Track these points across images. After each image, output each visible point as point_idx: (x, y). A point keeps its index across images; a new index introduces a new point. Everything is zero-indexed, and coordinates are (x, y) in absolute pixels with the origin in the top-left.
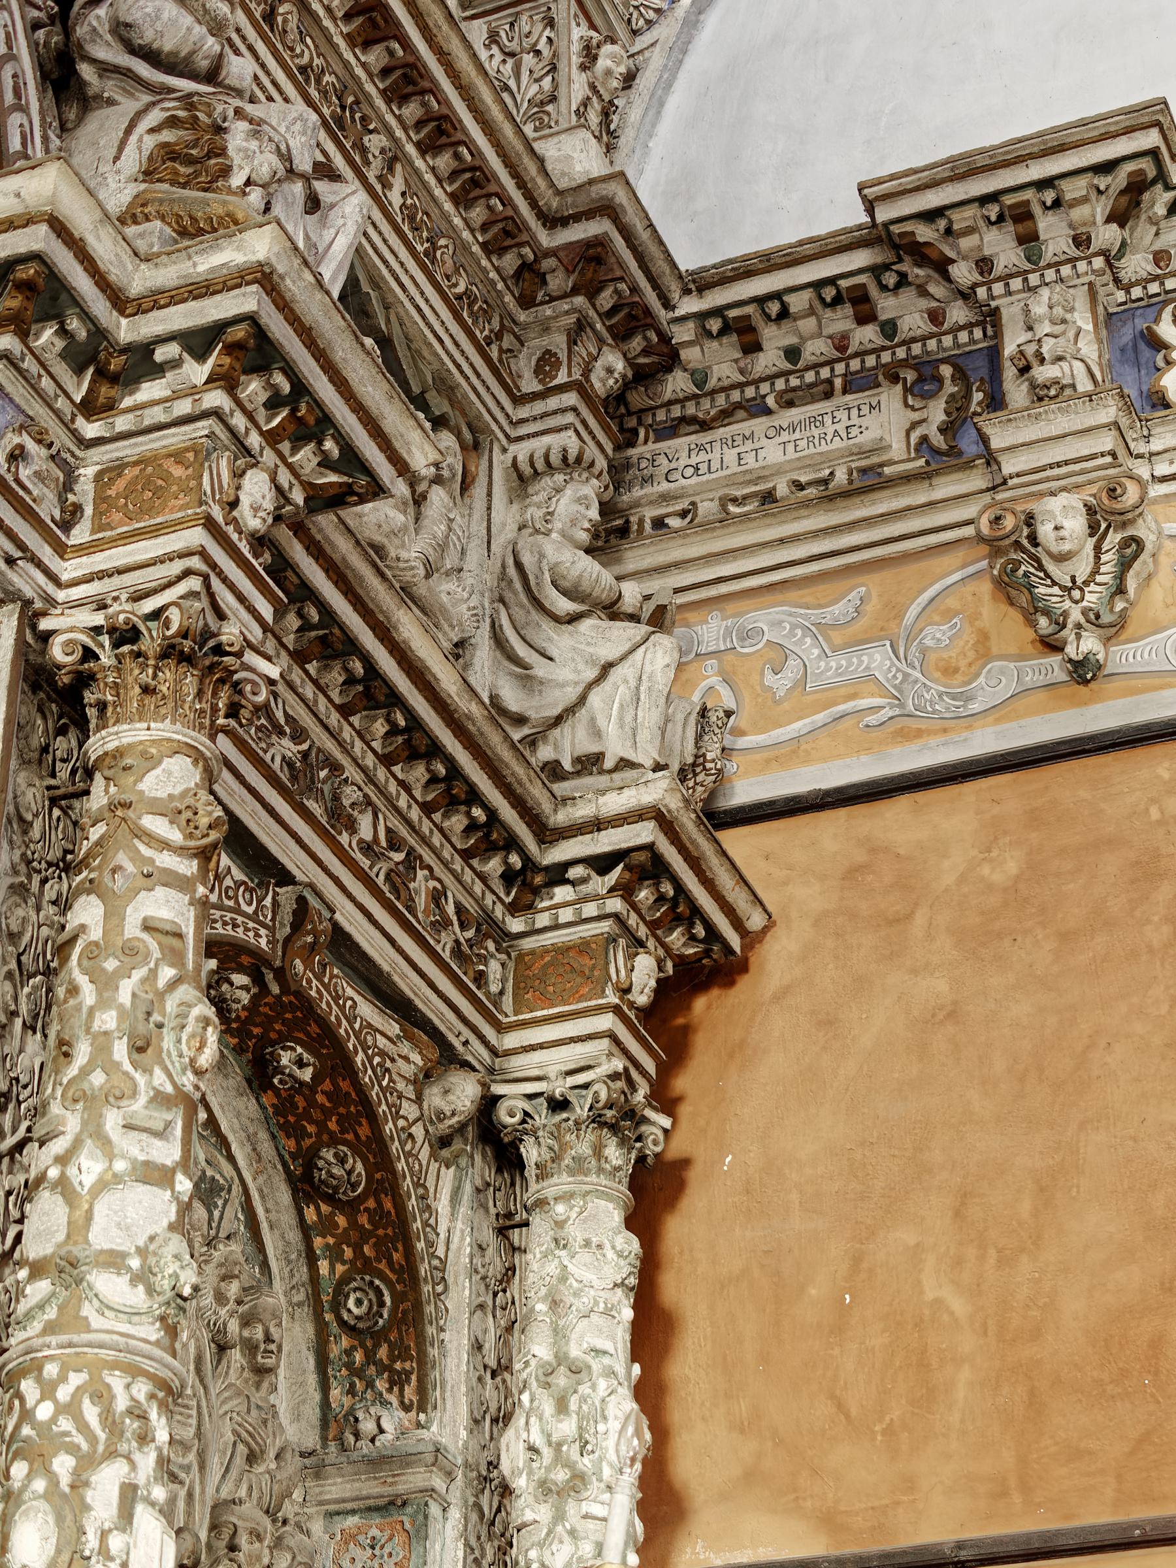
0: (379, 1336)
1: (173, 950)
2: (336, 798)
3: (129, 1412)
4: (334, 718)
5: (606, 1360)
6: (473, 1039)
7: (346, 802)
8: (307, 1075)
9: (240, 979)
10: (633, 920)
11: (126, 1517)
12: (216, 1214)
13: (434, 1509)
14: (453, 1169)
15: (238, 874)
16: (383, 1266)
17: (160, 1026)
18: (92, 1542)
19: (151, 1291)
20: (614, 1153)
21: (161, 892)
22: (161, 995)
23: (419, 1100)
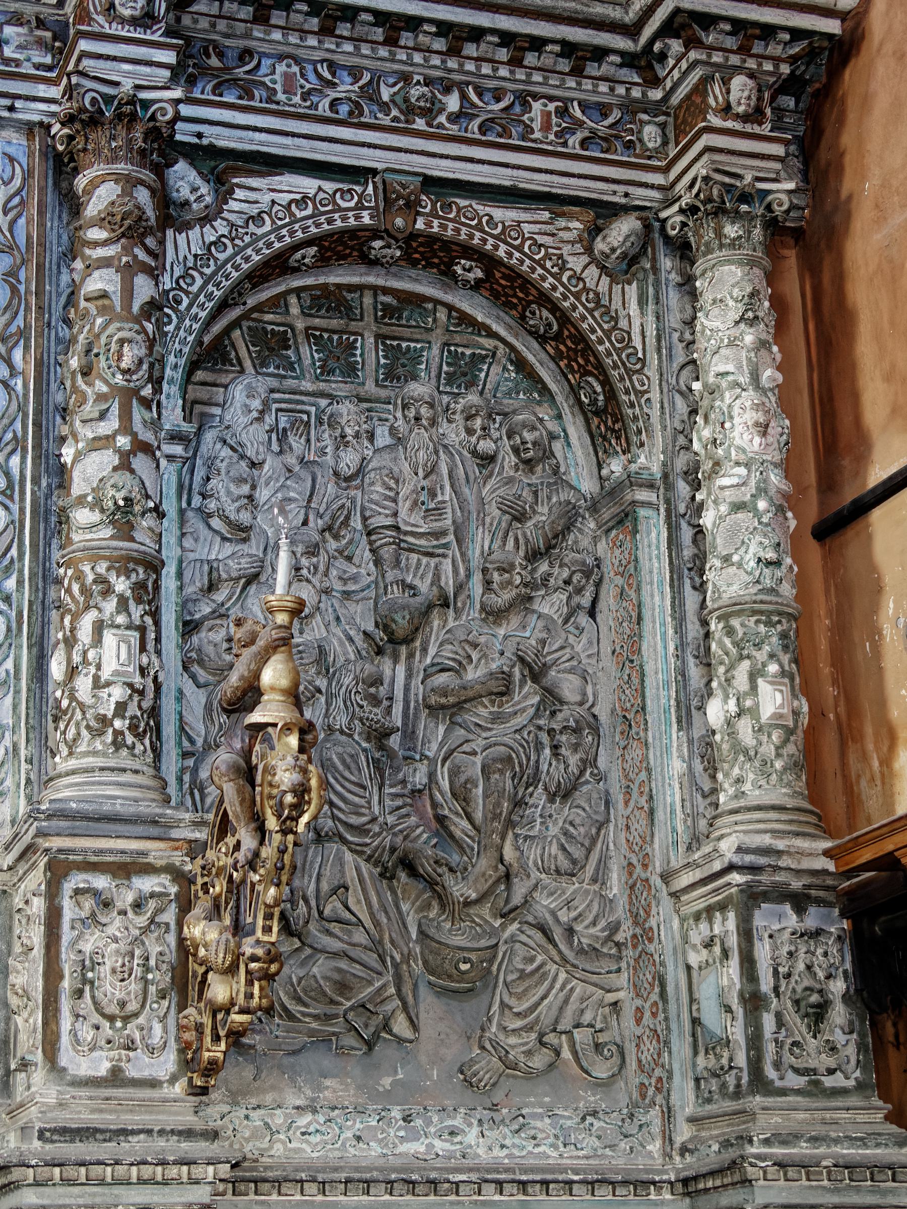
0: (605, 411)
1: (104, 307)
2: (406, 100)
3: (95, 581)
4: (383, 52)
5: (730, 378)
6: (631, 189)
7: (413, 100)
8: (479, 274)
9: (377, 244)
10: (717, 58)
11: (98, 640)
12: (483, 375)
13: (642, 512)
14: (635, 284)
15: (329, 186)
16: (590, 368)
17: (97, 355)
18: (77, 658)
19: (102, 511)
20: (731, 230)
21: (96, 274)
22: (98, 336)
23: (589, 250)
